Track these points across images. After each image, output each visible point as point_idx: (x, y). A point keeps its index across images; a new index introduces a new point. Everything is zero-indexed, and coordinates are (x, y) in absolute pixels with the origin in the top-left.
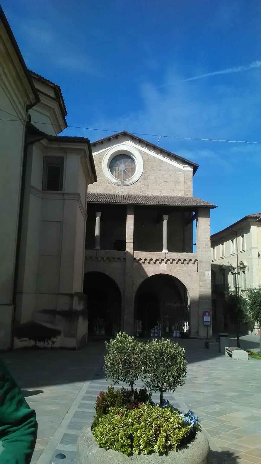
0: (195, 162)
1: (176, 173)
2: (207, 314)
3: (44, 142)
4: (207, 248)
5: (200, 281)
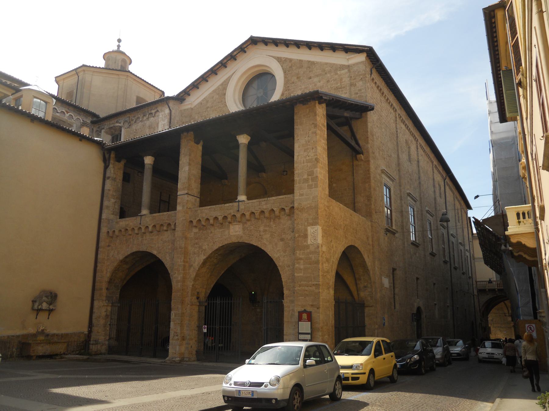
1: (336, 74)
2: (305, 316)
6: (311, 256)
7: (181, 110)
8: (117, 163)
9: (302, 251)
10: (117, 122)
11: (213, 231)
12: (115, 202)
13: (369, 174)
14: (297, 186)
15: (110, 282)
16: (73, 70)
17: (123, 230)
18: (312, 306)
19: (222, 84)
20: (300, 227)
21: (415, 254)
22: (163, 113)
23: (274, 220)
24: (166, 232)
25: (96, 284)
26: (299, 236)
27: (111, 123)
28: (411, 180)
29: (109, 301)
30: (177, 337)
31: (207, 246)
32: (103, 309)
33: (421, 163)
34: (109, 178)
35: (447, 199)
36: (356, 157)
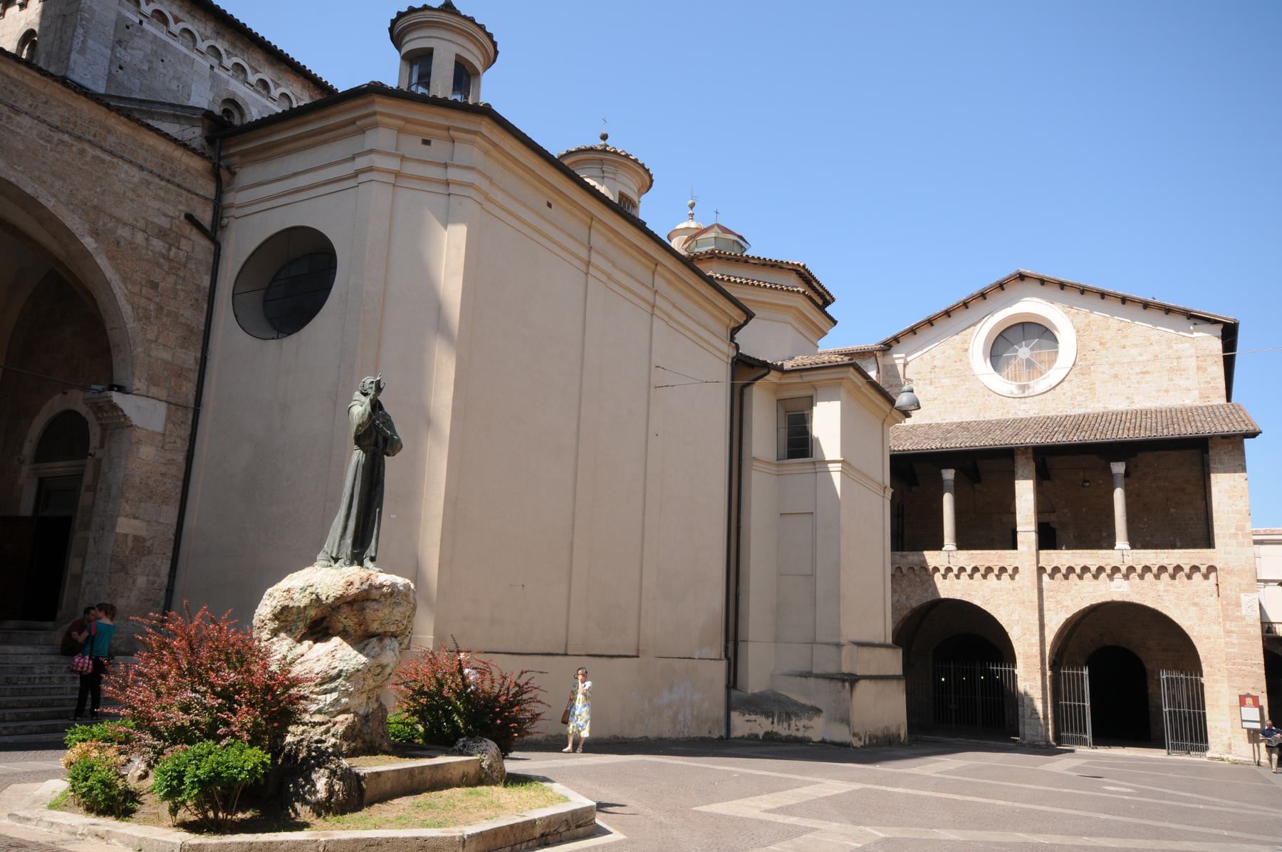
0: (1228, 315)
2: (1249, 701)
3: (773, 377)
5: (1227, 617)
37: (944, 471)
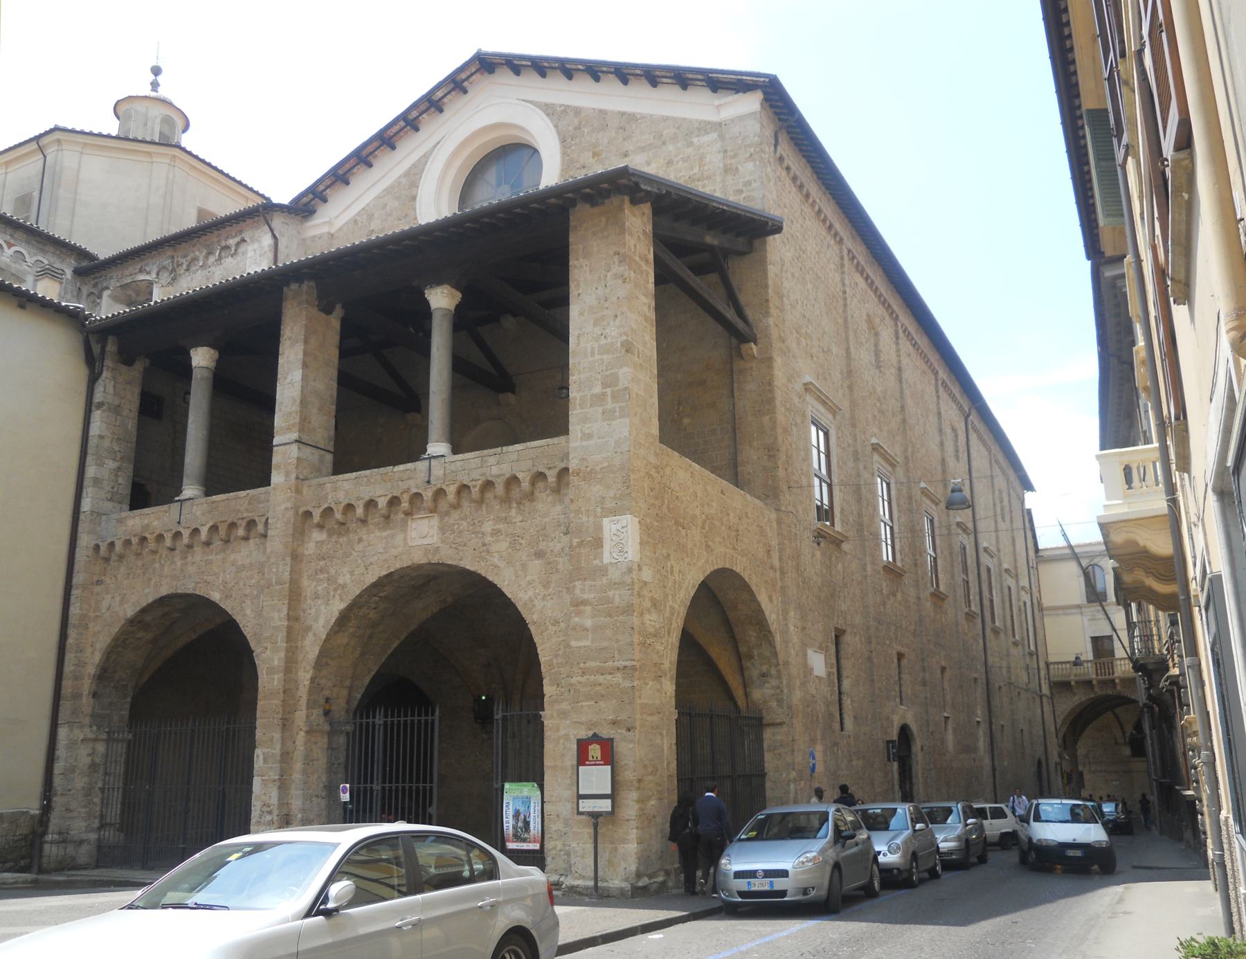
1: (690, 144)
2: (595, 751)
4: (609, 399)
6: (610, 593)
7: (304, 240)
8: (123, 368)
9: (588, 583)
10: (141, 271)
11: (364, 537)
12: (119, 469)
13: (771, 391)
14: (575, 414)
15: (103, 675)
16: (31, 140)
17: (135, 540)
18: (614, 723)
19: (407, 174)
20: (585, 519)
21: (894, 595)
22: (256, 246)
23: (519, 504)
24: (243, 543)
25: (64, 683)
26: (581, 544)
27: (127, 272)
28: (882, 412)
29: (99, 727)
30: (269, 818)
31: (348, 576)
32: (81, 749)
33: (907, 374)
34: (100, 405)
35: (974, 463)
36: (739, 349)
37: (192, 352)
